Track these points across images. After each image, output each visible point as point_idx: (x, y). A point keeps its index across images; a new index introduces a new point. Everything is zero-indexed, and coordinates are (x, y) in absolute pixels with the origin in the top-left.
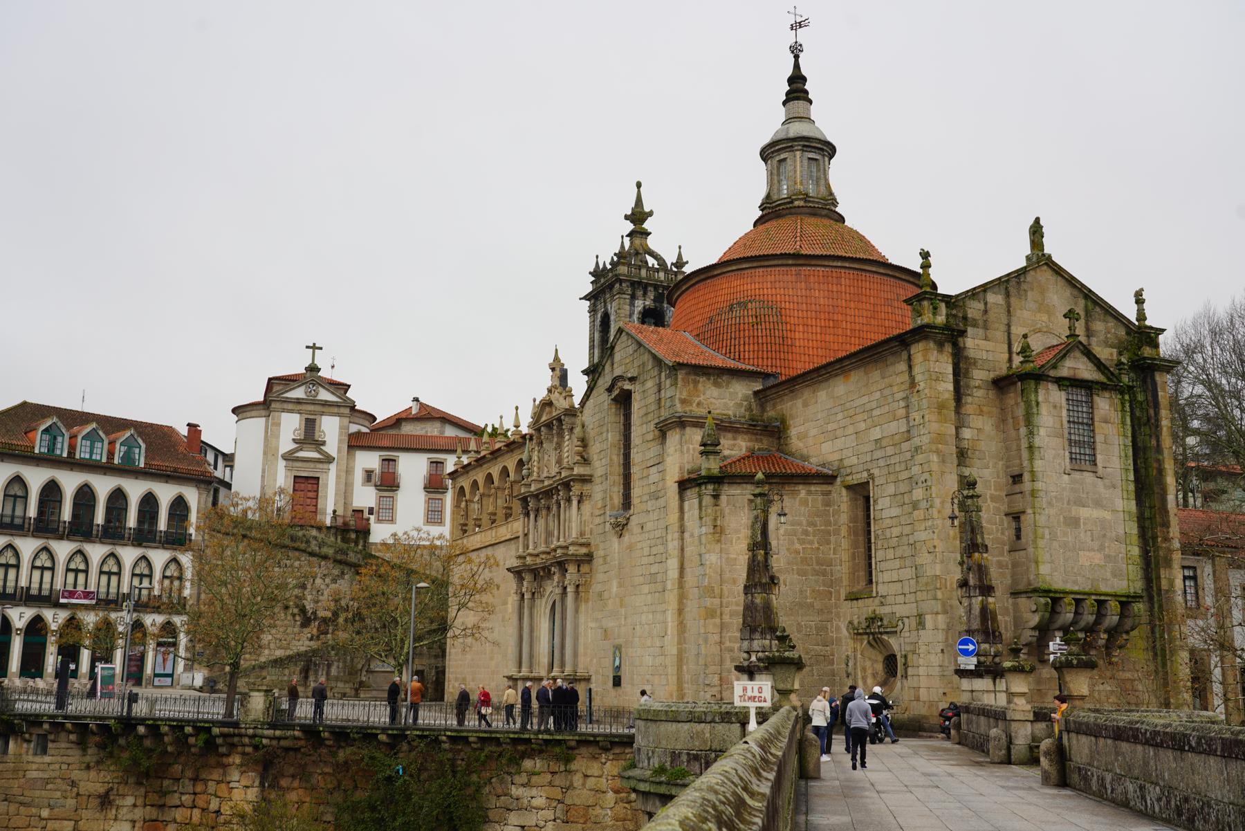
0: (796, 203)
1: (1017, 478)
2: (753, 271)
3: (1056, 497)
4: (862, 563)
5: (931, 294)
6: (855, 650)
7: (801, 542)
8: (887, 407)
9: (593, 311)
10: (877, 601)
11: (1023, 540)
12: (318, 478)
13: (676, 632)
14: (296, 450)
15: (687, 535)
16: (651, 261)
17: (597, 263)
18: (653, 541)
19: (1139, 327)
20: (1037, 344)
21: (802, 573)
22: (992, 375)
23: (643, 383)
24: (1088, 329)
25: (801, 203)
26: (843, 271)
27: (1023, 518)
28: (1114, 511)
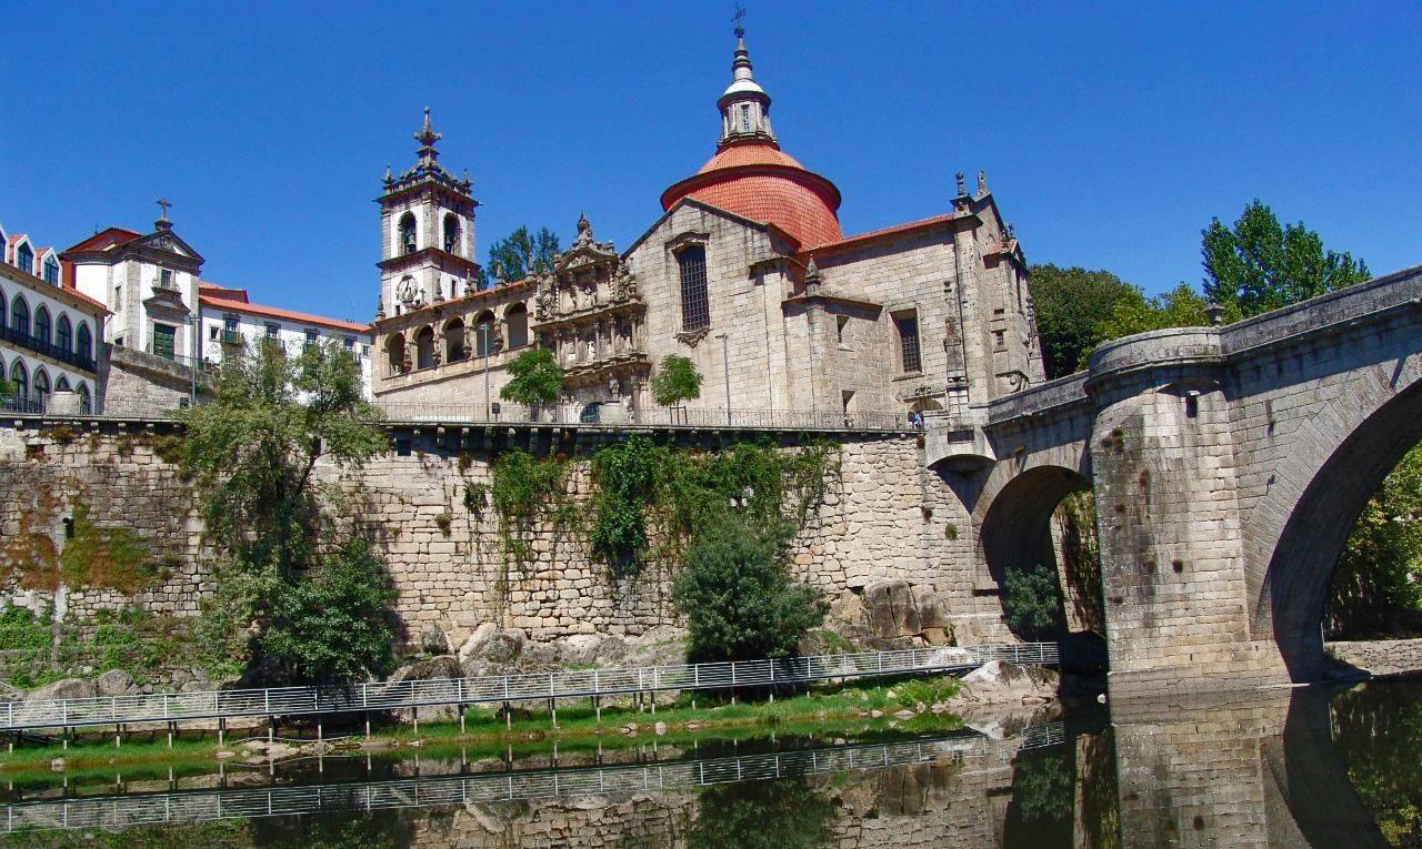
11: (1005, 345)
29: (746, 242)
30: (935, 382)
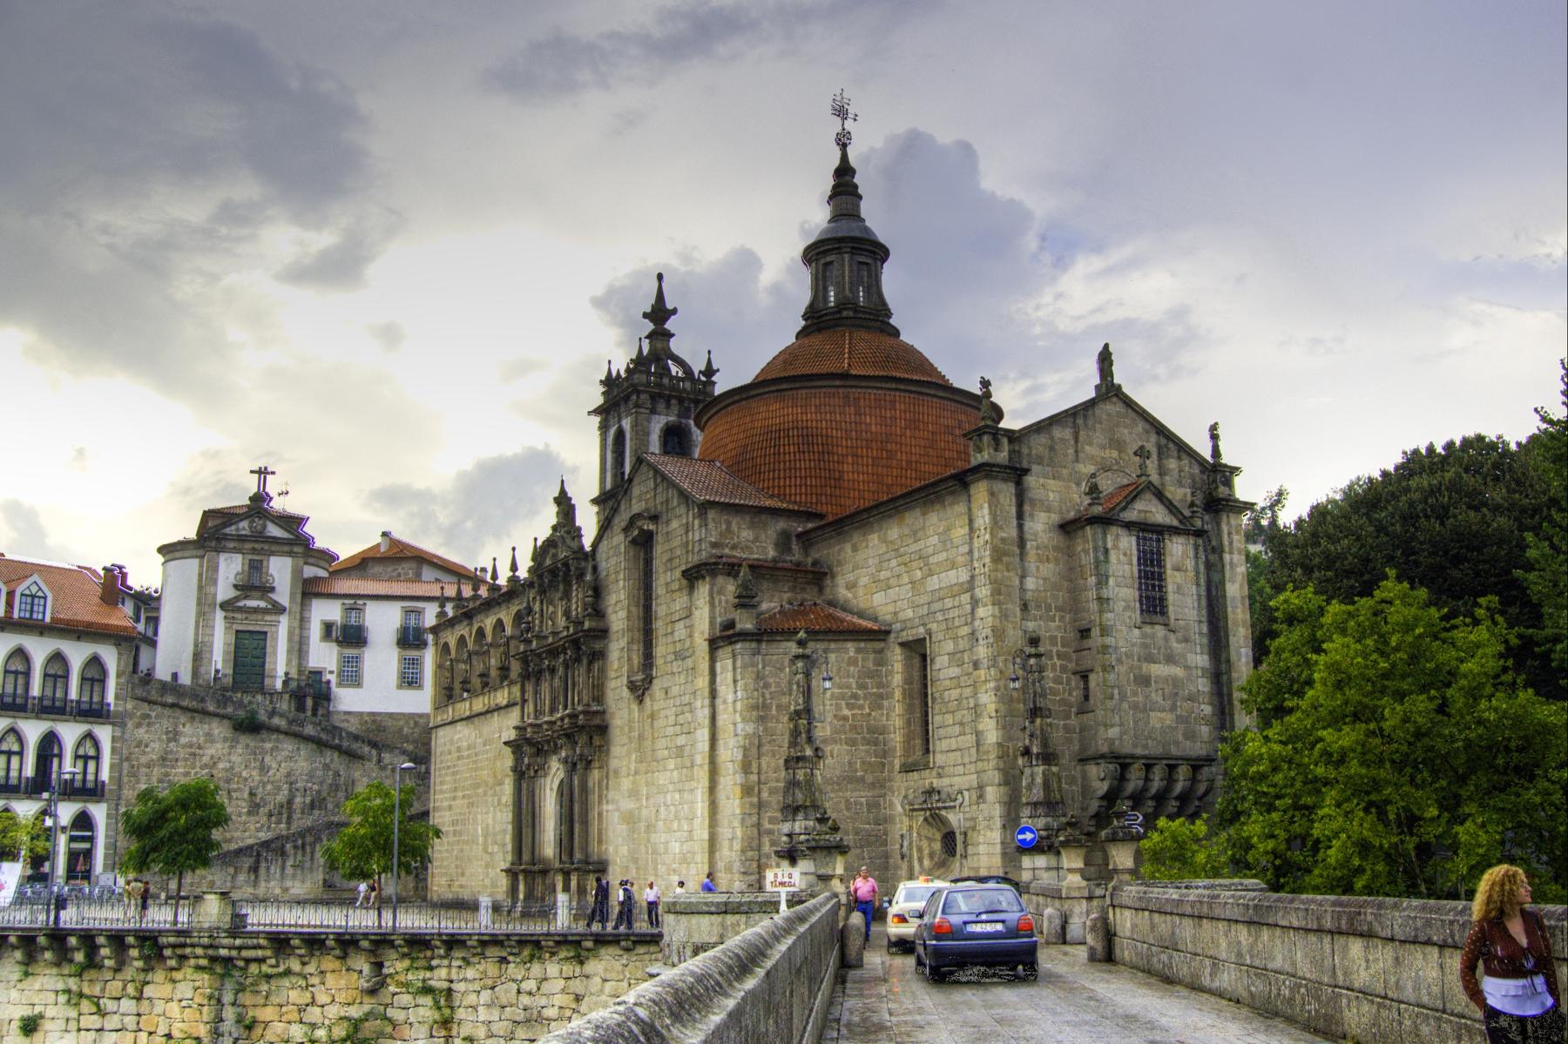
0: (845, 314)
1: (1085, 633)
2: (795, 392)
3: (1126, 654)
4: (918, 730)
5: (992, 427)
6: (911, 827)
7: (850, 707)
8: (945, 554)
9: (604, 428)
10: (934, 773)
11: (1092, 701)
12: (266, 633)
13: (706, 814)
14: (237, 599)
15: (719, 701)
16: (675, 370)
17: (609, 370)
18: (679, 709)
19: (1214, 466)
20: (1107, 484)
21: (852, 743)
22: (1055, 518)
23: (668, 523)
24: (1160, 466)
25: (851, 314)
26: (897, 393)
27: (1093, 678)
28: (1187, 668)
29: (687, 532)
30: (946, 781)
